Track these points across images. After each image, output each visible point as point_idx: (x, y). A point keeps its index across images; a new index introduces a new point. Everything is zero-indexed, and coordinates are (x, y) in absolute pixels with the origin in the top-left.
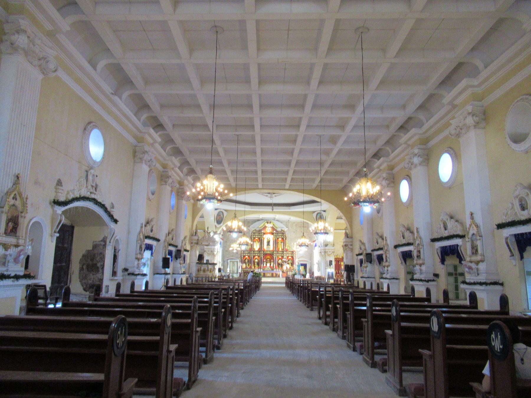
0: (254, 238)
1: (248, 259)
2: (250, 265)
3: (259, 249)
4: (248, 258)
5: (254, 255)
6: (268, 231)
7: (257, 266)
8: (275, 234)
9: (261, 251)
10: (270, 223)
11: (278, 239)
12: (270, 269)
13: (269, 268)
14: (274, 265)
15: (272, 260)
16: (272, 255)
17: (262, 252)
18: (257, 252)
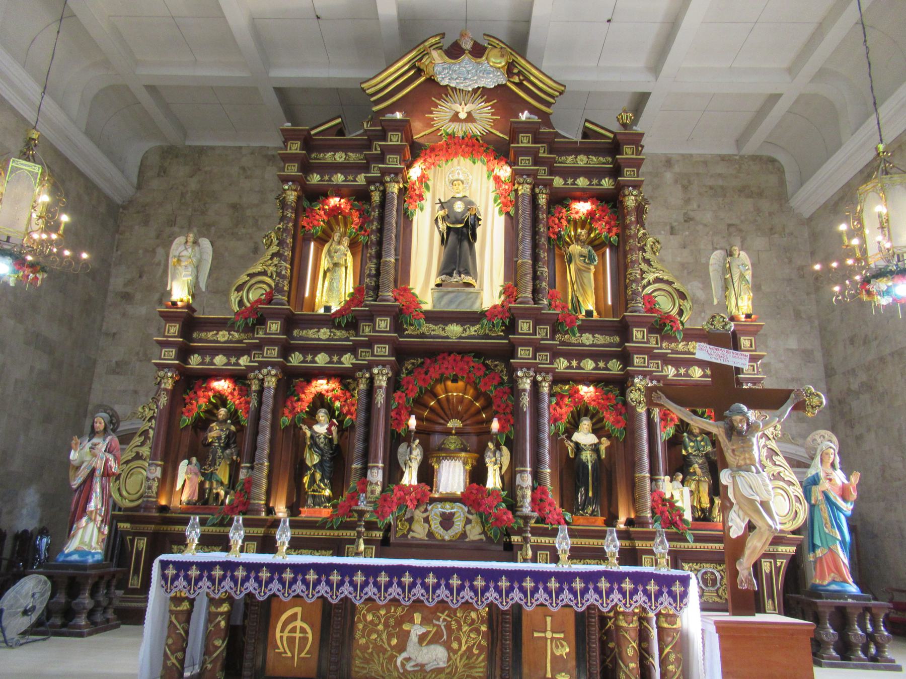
0: (315, 195)
1: (233, 416)
2: (243, 475)
3: (356, 297)
4: (234, 401)
5: (296, 359)
6: (458, 129)
7: (327, 492)
8: (525, 141)
9: (370, 317)
10: (478, 51)
11: (560, 200)
12: (475, 533)
13: (459, 511)
14: (526, 480)
15: (495, 425)
16: (501, 367)
17: (383, 324)
18: (324, 333)
